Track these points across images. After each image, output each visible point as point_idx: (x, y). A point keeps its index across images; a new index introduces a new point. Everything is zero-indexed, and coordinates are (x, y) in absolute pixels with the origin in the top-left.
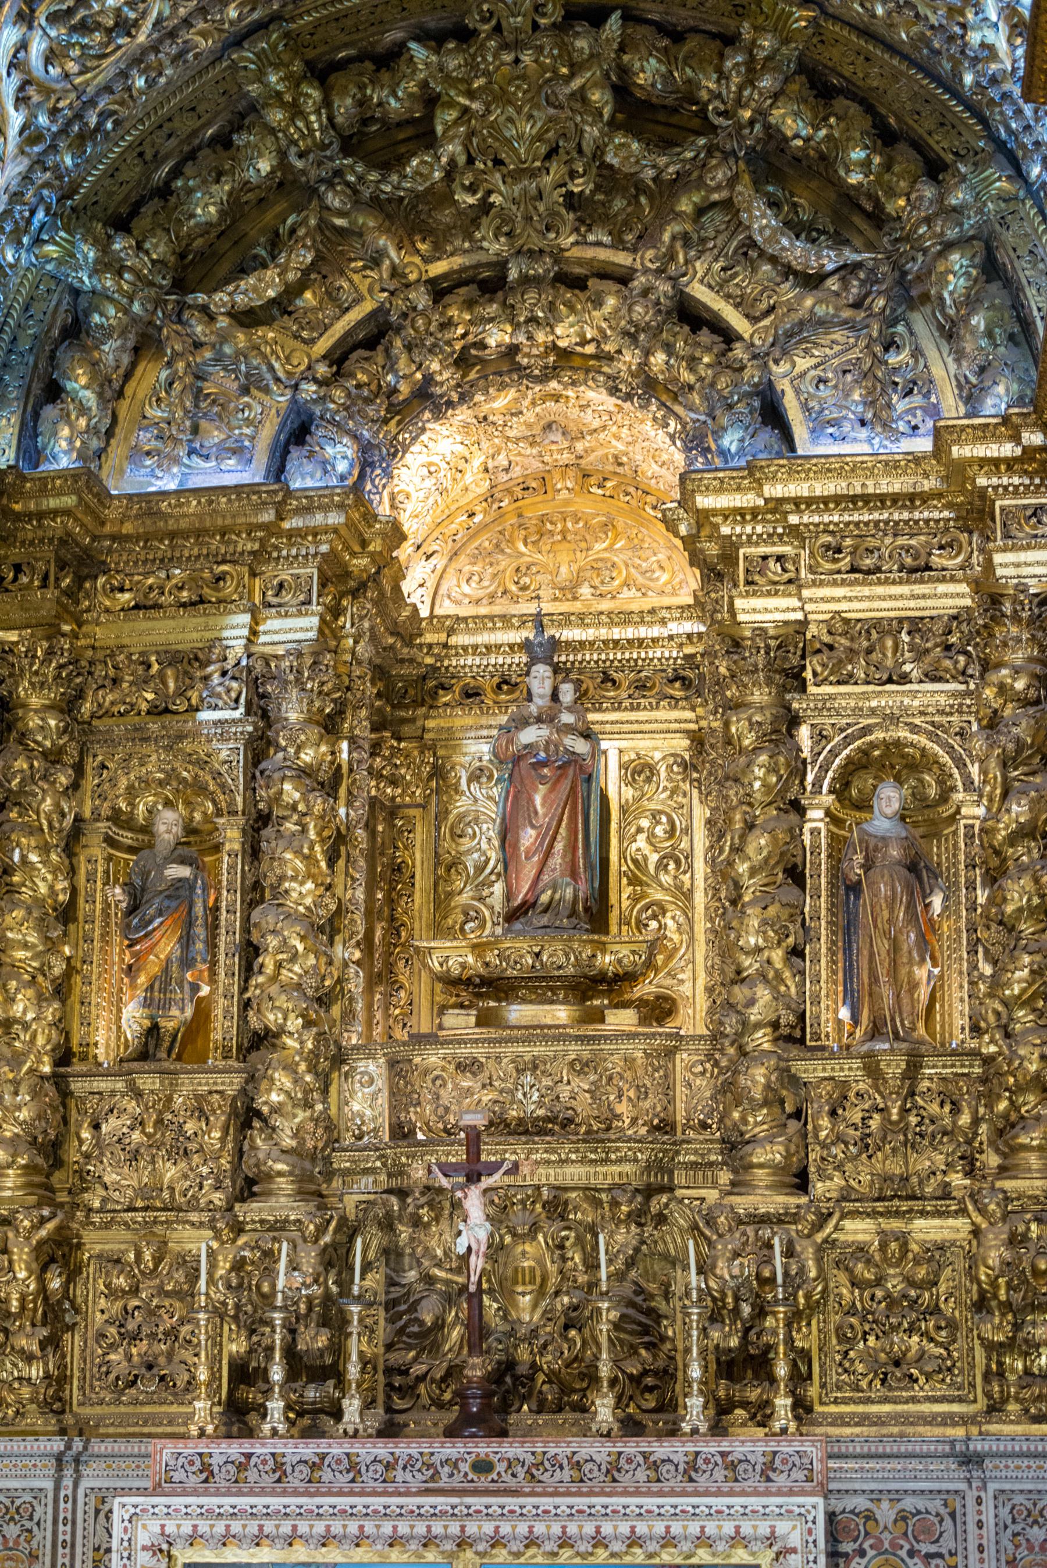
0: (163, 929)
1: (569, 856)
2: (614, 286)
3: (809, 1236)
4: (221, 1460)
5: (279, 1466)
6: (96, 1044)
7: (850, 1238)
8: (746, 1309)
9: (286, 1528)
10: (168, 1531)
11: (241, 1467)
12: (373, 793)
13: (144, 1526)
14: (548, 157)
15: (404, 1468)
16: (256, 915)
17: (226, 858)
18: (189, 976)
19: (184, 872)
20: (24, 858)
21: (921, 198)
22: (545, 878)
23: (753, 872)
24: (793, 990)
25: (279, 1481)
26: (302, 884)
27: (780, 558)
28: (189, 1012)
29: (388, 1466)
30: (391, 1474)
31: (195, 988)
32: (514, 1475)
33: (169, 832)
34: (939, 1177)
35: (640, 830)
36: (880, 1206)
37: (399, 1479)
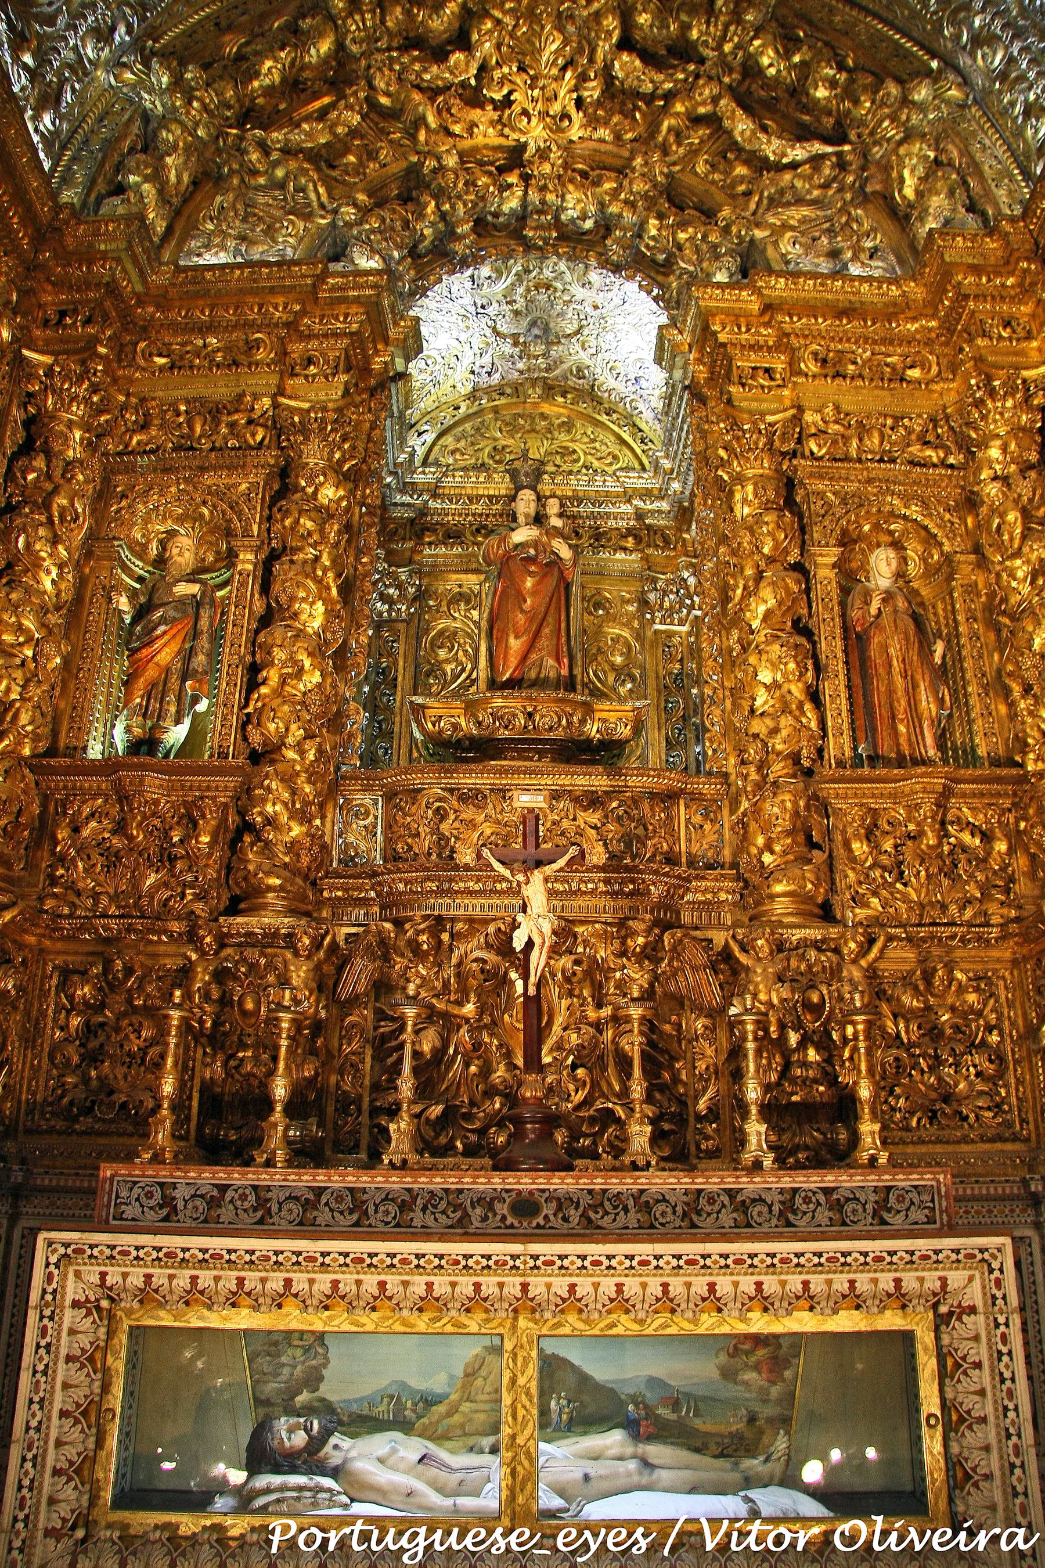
0: (166, 638)
2: (613, 175)
3: (854, 962)
4: (189, 1193)
8: (793, 1038)
11: (214, 1203)
13: (78, 1274)
14: (564, 69)
15: (424, 1209)
16: (261, 638)
19: (195, 589)
20: (28, 546)
21: (889, 94)
22: (534, 656)
23: (767, 616)
24: (813, 725)
27: (767, 370)
29: (405, 1207)
32: (565, 1219)
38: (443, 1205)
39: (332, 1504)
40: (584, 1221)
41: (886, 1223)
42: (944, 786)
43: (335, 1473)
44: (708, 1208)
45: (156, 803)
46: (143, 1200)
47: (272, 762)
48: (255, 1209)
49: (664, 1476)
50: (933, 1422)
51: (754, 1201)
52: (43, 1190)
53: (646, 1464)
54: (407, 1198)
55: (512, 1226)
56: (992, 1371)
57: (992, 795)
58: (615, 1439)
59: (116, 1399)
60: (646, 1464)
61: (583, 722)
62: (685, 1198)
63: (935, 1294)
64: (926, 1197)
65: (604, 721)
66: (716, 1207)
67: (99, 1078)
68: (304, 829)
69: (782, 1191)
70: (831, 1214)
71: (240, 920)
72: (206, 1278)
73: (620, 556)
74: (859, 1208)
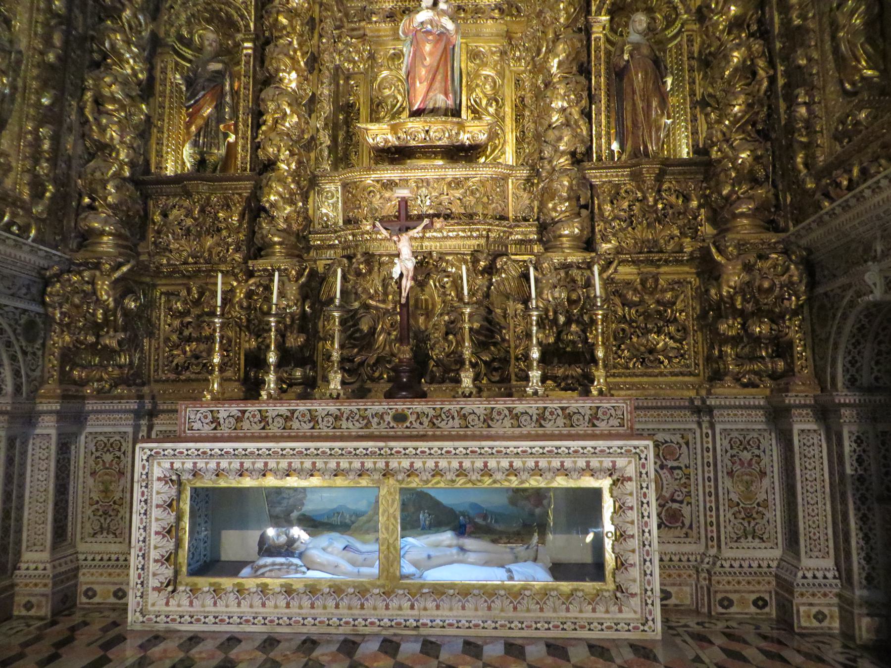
1: (443, 84)
4: (225, 415)
5: (264, 419)
6: (166, 168)
7: (621, 277)
9: (260, 465)
10: (176, 466)
11: (239, 420)
12: (338, 63)
13: (159, 464)
15: (347, 419)
16: (263, 95)
17: (243, 58)
18: (221, 126)
22: (431, 94)
24: (585, 132)
25: (263, 428)
26: (289, 73)
28: (223, 151)
29: (337, 418)
30: (338, 424)
31: (226, 136)
32: (421, 423)
33: (211, 45)
34: (676, 239)
35: (477, 85)
36: (642, 257)
37: (344, 426)
38: (357, 417)
39: (297, 572)
40: (431, 424)
41: (596, 426)
42: (660, 169)
43: (301, 556)
44: (497, 417)
45: (208, 198)
46: (203, 420)
47: (273, 170)
48: (260, 422)
49: (471, 557)
50: (610, 535)
51: (522, 413)
52: (164, 411)
53: (462, 549)
54: (338, 413)
55: (393, 427)
56: (638, 512)
57: (691, 173)
58: (447, 537)
59: (186, 524)
60: (462, 549)
61: (458, 134)
62: (485, 412)
63: (609, 470)
64: (619, 412)
65: (471, 132)
66: (502, 417)
67: (191, 351)
68: (293, 208)
69: (538, 409)
70: (565, 421)
71: (261, 261)
72: (224, 464)
73: (490, 22)
74: (581, 418)
